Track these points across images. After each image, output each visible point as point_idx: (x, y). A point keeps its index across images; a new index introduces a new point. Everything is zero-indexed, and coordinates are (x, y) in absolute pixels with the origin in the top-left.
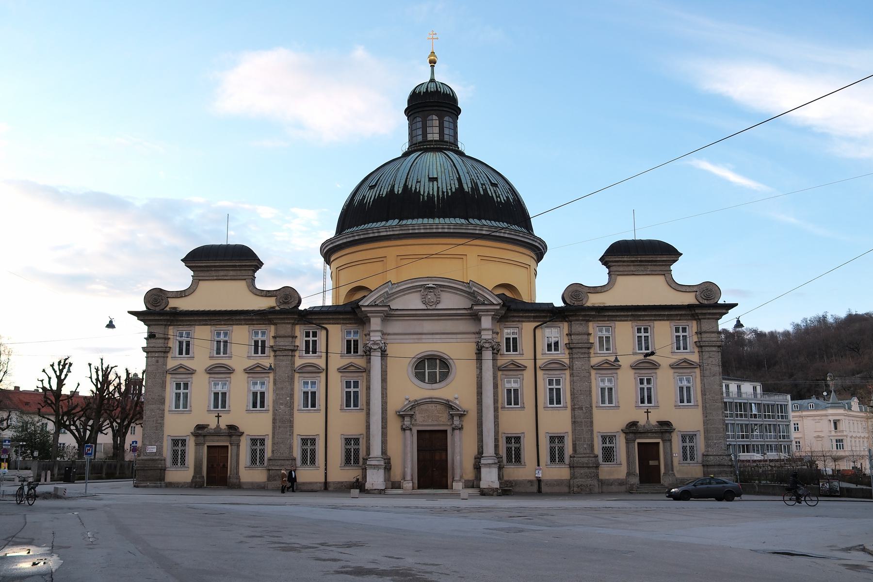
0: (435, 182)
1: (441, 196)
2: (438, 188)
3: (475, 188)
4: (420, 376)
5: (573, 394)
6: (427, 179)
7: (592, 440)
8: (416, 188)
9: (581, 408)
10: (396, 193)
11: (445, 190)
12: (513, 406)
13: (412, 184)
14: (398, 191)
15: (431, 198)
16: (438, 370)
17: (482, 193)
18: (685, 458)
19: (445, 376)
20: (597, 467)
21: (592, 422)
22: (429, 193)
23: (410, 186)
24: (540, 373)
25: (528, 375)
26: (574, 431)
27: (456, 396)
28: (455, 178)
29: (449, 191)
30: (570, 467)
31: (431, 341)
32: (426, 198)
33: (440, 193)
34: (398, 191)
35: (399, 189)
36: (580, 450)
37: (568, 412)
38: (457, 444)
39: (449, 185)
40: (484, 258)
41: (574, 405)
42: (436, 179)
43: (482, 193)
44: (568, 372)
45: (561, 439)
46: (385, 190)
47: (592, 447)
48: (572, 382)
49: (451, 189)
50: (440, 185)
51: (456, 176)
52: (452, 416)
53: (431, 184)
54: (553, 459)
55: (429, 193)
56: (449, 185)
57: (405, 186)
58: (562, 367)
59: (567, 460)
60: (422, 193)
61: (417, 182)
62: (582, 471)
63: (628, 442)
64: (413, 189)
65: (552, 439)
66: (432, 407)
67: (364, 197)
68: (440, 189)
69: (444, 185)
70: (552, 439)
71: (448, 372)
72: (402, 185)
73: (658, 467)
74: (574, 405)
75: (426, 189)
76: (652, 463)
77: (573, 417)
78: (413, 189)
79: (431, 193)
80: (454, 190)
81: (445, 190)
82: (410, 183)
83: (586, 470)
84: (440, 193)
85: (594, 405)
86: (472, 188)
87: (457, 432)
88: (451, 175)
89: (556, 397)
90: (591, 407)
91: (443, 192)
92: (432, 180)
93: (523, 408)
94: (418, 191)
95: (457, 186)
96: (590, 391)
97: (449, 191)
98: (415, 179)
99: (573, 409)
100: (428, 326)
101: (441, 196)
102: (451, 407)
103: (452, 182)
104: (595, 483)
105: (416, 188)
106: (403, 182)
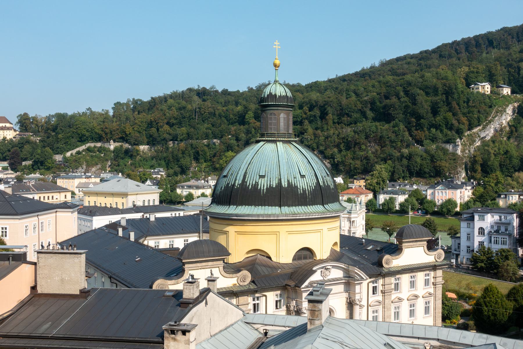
0: (304, 178)
2: (307, 183)
8: (295, 183)
10: (284, 186)
14: (285, 185)
29: (313, 185)
32: (302, 191)
33: (309, 188)
34: (285, 185)
49: (313, 184)
53: (303, 180)
55: (303, 187)
57: (288, 181)
60: (299, 187)
61: (294, 178)
72: (286, 181)
78: (293, 183)
79: (304, 188)
80: (315, 185)
81: (311, 185)
82: (290, 179)
84: (309, 188)
97: (313, 185)
101: (309, 190)
105: (295, 183)
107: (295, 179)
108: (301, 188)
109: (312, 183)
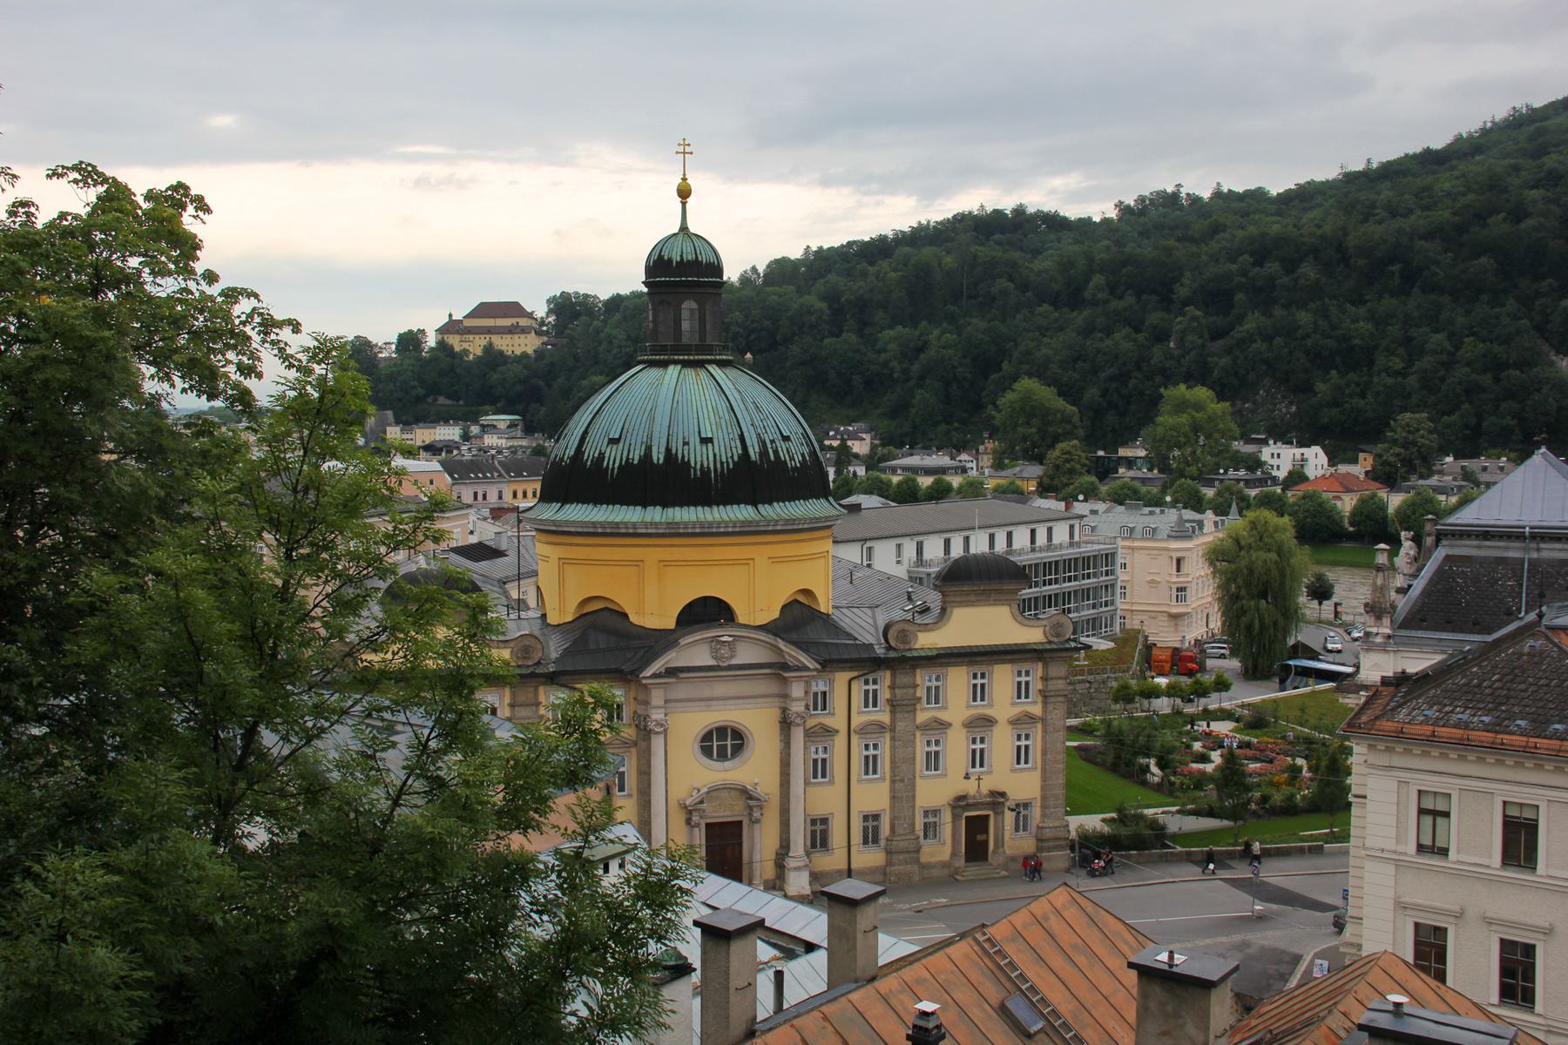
0: (710, 445)
1: (719, 470)
2: (715, 455)
3: (764, 453)
4: (707, 751)
5: (893, 762)
6: (698, 440)
7: (914, 815)
8: (683, 456)
9: (902, 780)
10: (656, 462)
11: (724, 460)
12: (820, 779)
13: (677, 447)
14: (658, 459)
15: (705, 472)
16: (729, 742)
17: (772, 458)
18: (1017, 829)
19: (738, 749)
20: (918, 851)
21: (914, 796)
22: (702, 465)
23: (674, 451)
24: (854, 739)
25: (840, 742)
26: (892, 808)
27: (756, 781)
28: (737, 437)
29: (730, 460)
30: (887, 853)
31: (723, 707)
32: (699, 473)
33: (719, 466)
34: (658, 459)
35: (658, 456)
36: (899, 831)
37: (886, 785)
38: (757, 840)
39: (729, 450)
40: (775, 560)
41: (895, 776)
42: (710, 440)
43: (772, 458)
44: (888, 736)
45: (876, 817)
46: (637, 452)
47: (913, 824)
48: (893, 748)
49: (732, 457)
50: (717, 450)
51: (737, 432)
52: (751, 808)
54: (865, 842)
55: (702, 465)
56: (729, 450)
57: (668, 450)
58: (881, 727)
59: (882, 843)
60: (693, 465)
62: (901, 857)
63: (955, 818)
64: (680, 456)
65: (866, 818)
66: (725, 794)
67: (602, 455)
68: (718, 458)
69: (722, 448)
70: (866, 818)
71: (742, 744)
72: (663, 450)
73: (986, 842)
74: (895, 776)
75: (698, 457)
76: (980, 837)
77: (893, 790)
78: (680, 456)
79: (705, 465)
80: (736, 459)
81: (724, 460)
82: (674, 445)
83: (907, 856)
84: (719, 466)
85: (917, 775)
86: (761, 454)
87: (757, 826)
88: (730, 431)
89: (871, 764)
90: (914, 777)
91: (722, 463)
92: (706, 441)
93: (832, 782)
94: (686, 459)
95: (740, 452)
96: (914, 758)
97: (730, 460)
98: (681, 437)
99: (893, 782)
100: (720, 689)
101: (719, 470)
102: (751, 797)
103: (733, 444)
104: (916, 867)
105: (683, 456)
106: (665, 445)
107: (686, 447)
108: (698, 467)
109: (729, 455)
